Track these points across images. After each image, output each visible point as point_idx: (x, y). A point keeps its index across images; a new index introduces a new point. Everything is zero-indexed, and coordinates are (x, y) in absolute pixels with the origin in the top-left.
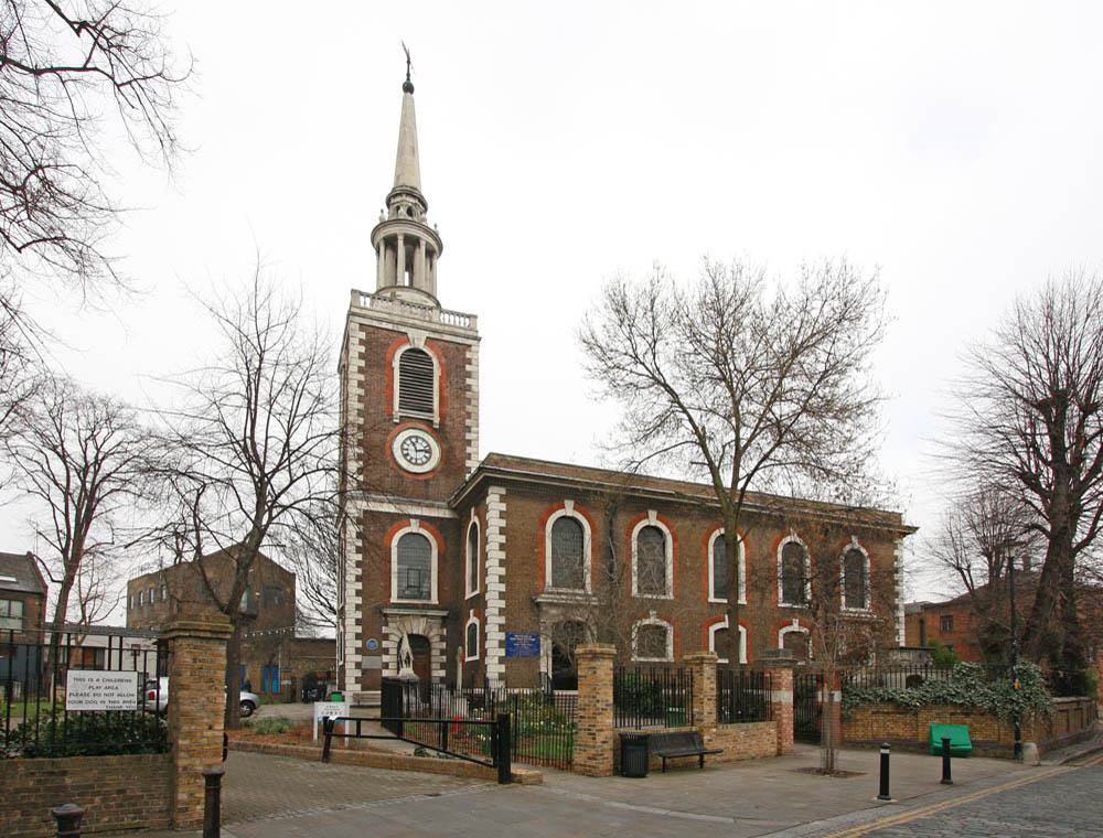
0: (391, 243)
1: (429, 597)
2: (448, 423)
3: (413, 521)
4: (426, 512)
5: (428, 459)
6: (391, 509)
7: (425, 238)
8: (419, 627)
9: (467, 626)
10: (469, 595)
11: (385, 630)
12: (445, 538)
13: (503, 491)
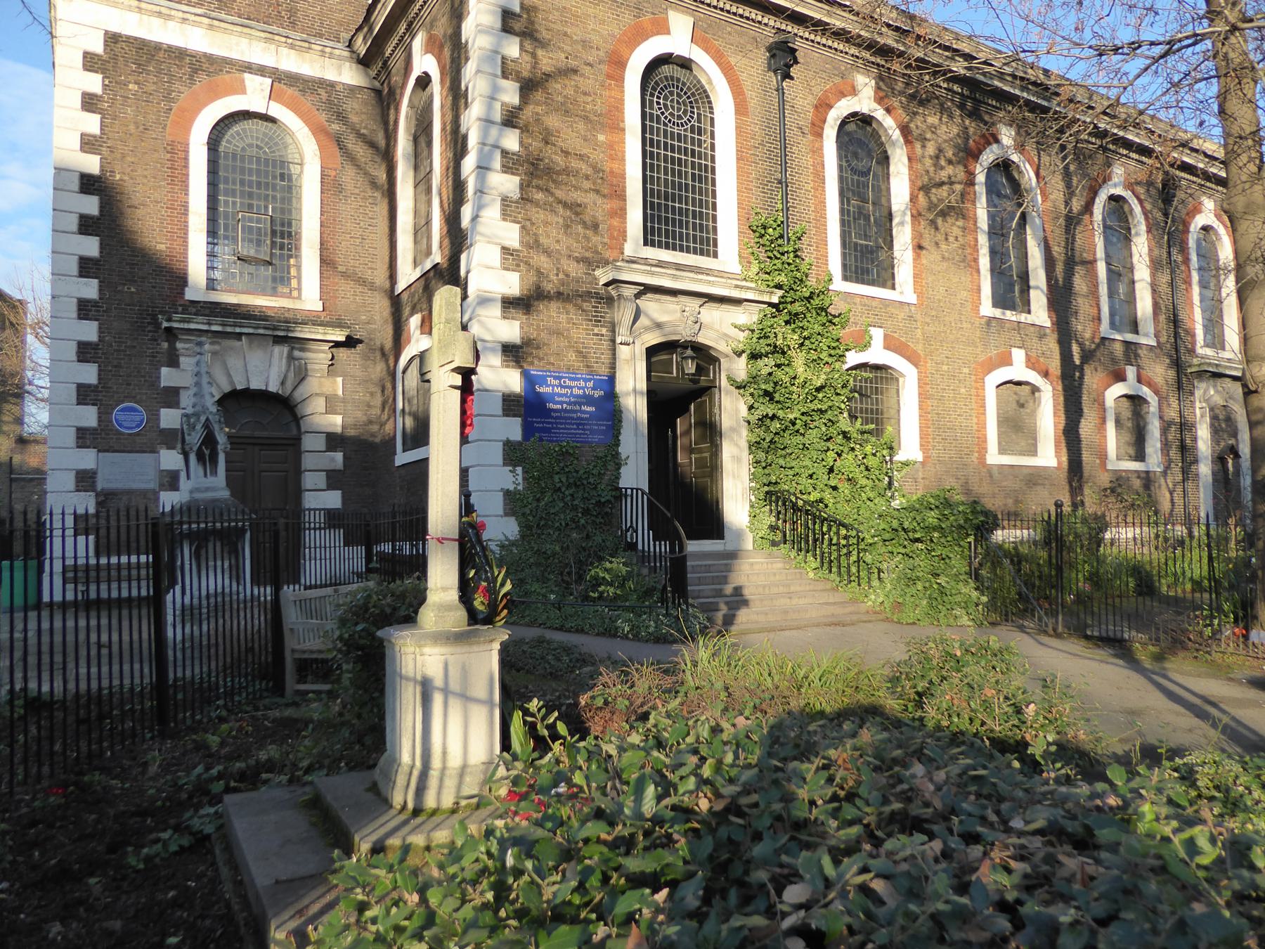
3: (251, 80)
11: (167, 376)
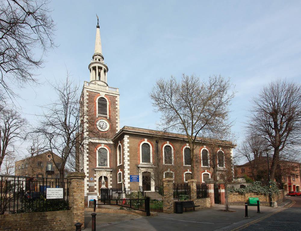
0: (94, 68)
1: (107, 166)
2: (111, 117)
4: (106, 142)
5: (106, 128)
6: (97, 141)
7: (104, 67)
8: (104, 174)
9: (118, 174)
10: (118, 165)
11: (95, 175)
12: (111, 149)
13: (128, 136)
